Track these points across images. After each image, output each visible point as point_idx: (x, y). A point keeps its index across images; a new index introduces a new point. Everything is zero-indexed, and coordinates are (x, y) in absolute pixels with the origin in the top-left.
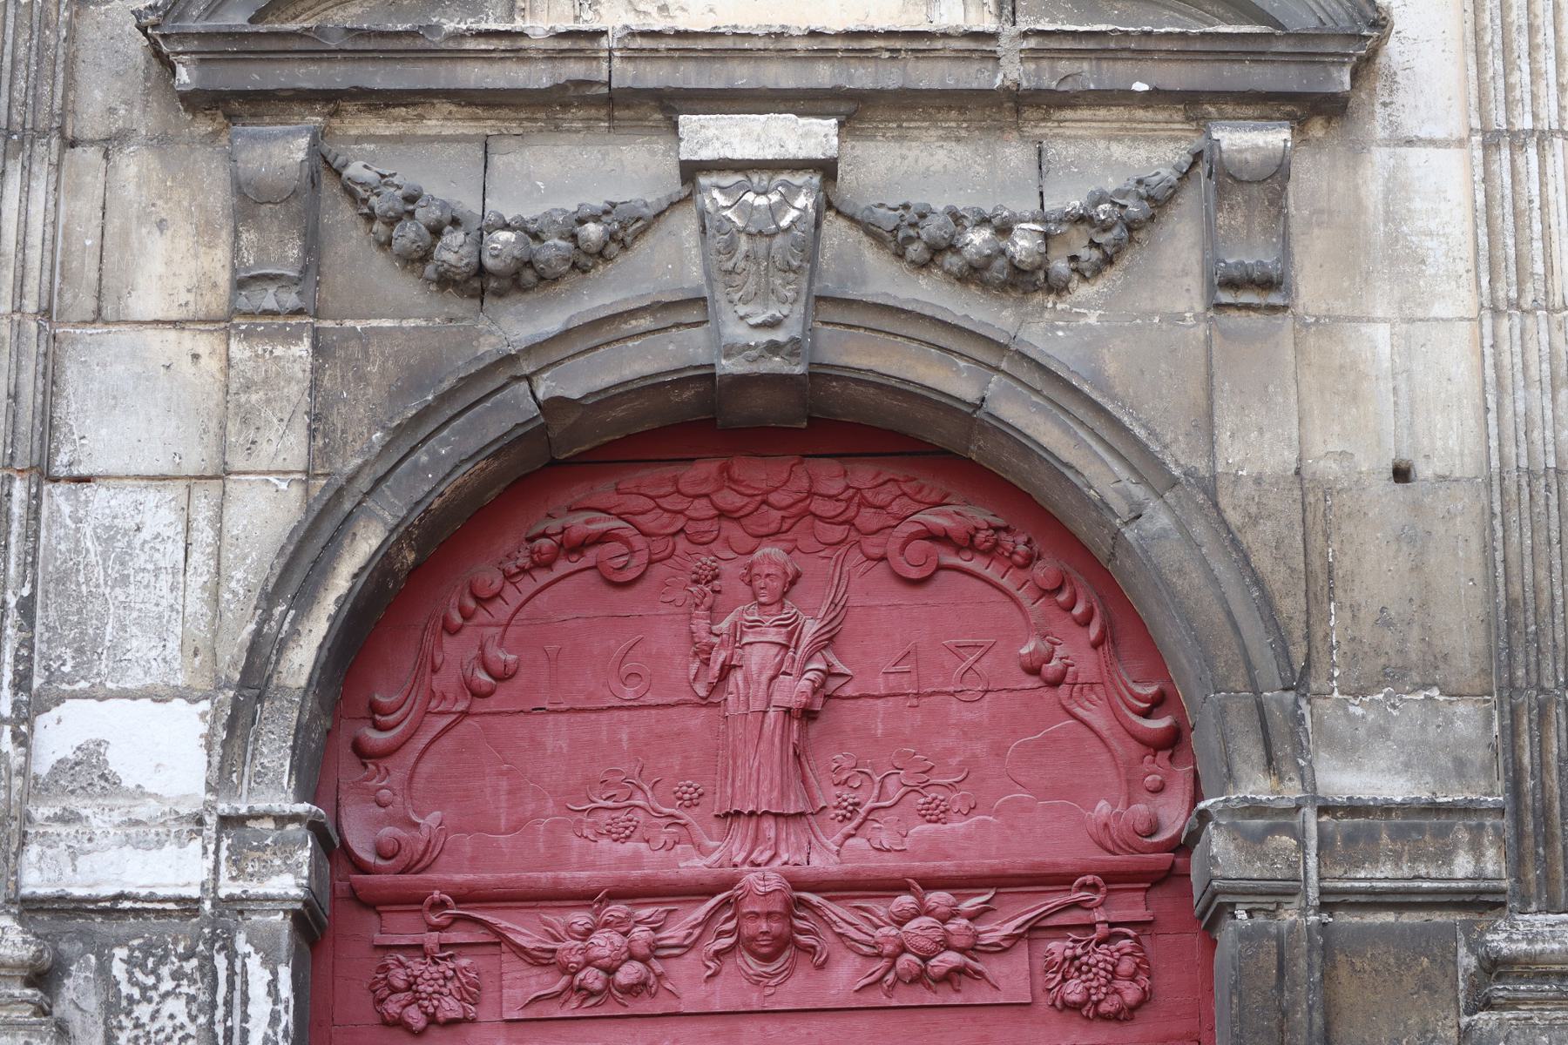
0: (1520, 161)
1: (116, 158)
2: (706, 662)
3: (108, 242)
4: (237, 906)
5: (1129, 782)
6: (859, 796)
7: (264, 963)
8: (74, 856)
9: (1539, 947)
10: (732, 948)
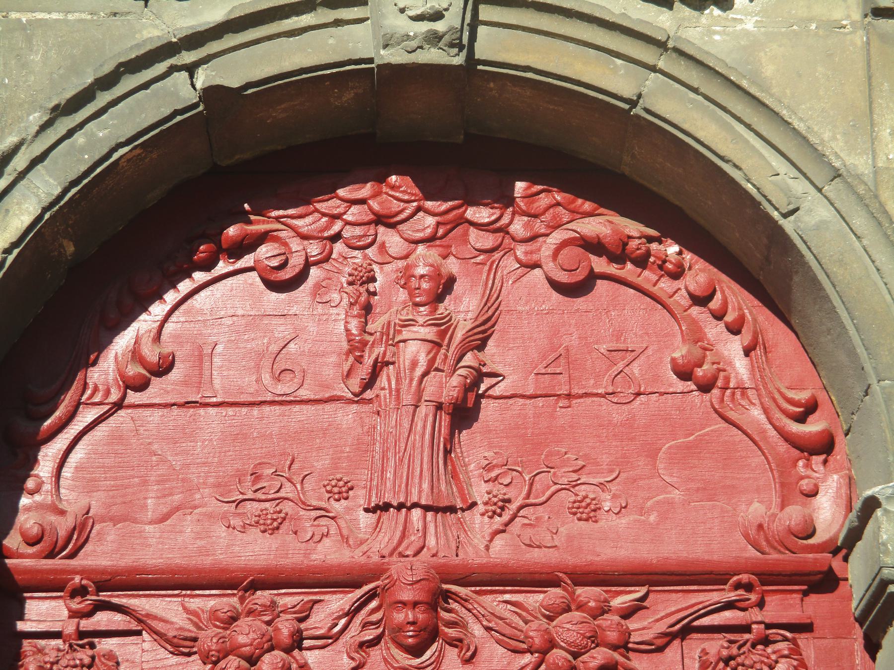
2: (359, 360)
5: (782, 485)
6: (511, 493)
10: (375, 642)
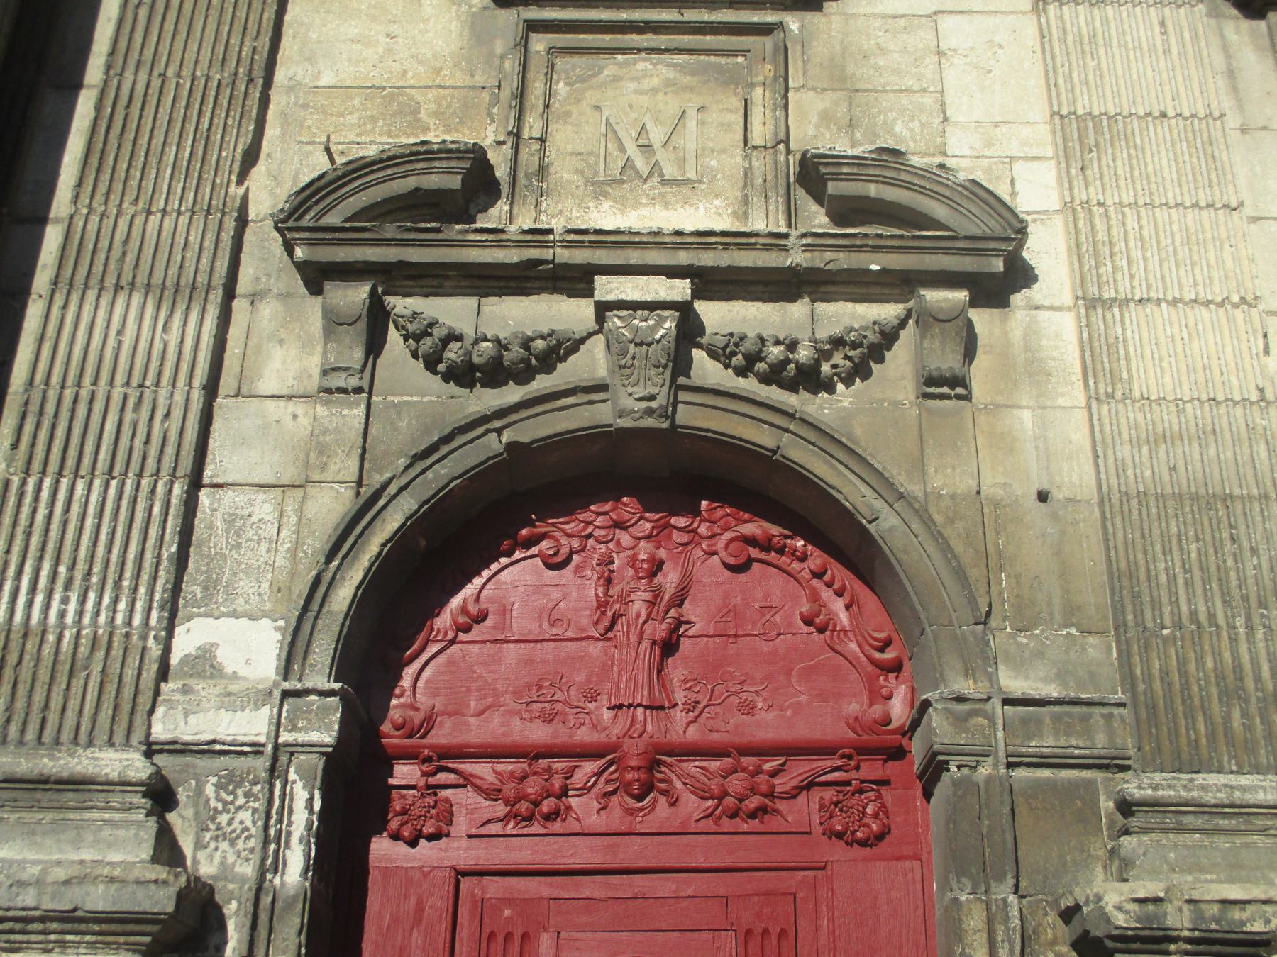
0: (1109, 316)
1: (259, 305)
2: (604, 613)
3: (248, 352)
4: (294, 749)
5: (870, 692)
6: (699, 697)
7: (305, 787)
8: (186, 714)
9: (1160, 793)
10: (614, 792)
